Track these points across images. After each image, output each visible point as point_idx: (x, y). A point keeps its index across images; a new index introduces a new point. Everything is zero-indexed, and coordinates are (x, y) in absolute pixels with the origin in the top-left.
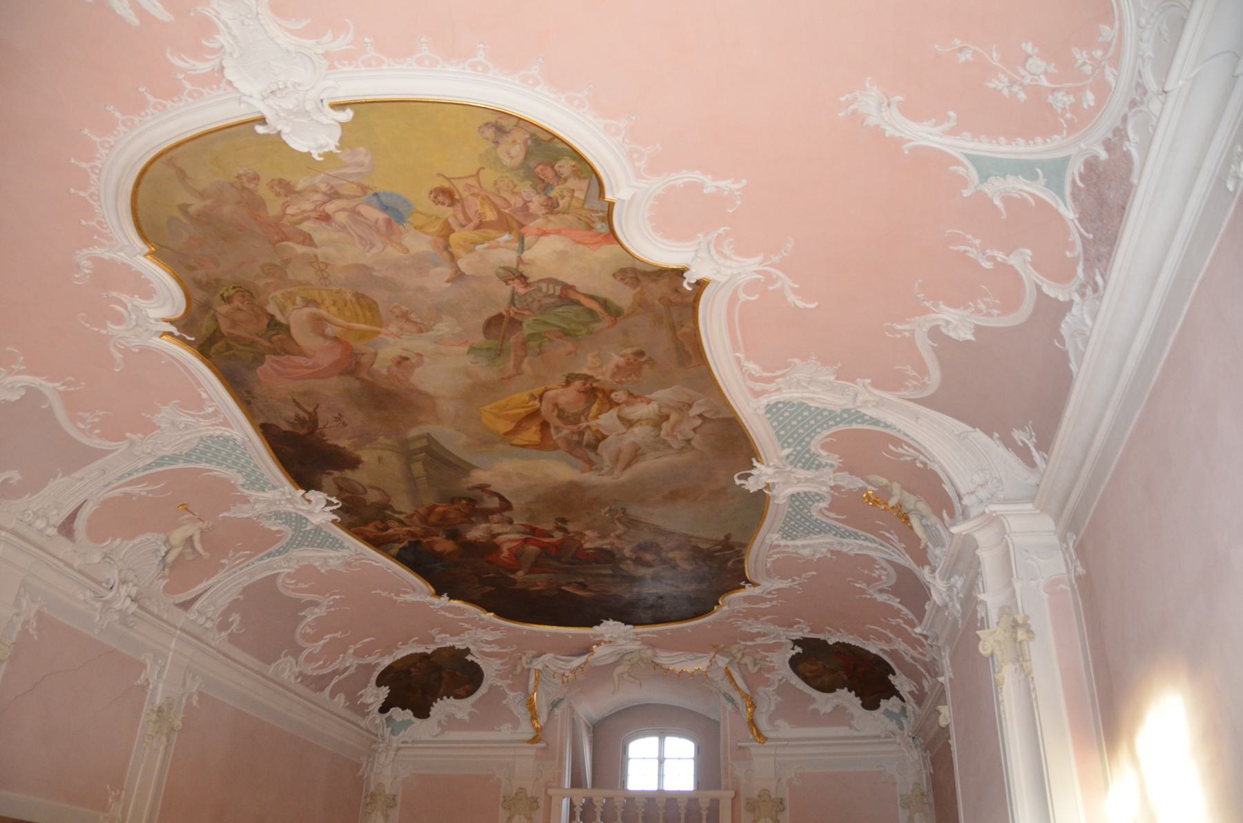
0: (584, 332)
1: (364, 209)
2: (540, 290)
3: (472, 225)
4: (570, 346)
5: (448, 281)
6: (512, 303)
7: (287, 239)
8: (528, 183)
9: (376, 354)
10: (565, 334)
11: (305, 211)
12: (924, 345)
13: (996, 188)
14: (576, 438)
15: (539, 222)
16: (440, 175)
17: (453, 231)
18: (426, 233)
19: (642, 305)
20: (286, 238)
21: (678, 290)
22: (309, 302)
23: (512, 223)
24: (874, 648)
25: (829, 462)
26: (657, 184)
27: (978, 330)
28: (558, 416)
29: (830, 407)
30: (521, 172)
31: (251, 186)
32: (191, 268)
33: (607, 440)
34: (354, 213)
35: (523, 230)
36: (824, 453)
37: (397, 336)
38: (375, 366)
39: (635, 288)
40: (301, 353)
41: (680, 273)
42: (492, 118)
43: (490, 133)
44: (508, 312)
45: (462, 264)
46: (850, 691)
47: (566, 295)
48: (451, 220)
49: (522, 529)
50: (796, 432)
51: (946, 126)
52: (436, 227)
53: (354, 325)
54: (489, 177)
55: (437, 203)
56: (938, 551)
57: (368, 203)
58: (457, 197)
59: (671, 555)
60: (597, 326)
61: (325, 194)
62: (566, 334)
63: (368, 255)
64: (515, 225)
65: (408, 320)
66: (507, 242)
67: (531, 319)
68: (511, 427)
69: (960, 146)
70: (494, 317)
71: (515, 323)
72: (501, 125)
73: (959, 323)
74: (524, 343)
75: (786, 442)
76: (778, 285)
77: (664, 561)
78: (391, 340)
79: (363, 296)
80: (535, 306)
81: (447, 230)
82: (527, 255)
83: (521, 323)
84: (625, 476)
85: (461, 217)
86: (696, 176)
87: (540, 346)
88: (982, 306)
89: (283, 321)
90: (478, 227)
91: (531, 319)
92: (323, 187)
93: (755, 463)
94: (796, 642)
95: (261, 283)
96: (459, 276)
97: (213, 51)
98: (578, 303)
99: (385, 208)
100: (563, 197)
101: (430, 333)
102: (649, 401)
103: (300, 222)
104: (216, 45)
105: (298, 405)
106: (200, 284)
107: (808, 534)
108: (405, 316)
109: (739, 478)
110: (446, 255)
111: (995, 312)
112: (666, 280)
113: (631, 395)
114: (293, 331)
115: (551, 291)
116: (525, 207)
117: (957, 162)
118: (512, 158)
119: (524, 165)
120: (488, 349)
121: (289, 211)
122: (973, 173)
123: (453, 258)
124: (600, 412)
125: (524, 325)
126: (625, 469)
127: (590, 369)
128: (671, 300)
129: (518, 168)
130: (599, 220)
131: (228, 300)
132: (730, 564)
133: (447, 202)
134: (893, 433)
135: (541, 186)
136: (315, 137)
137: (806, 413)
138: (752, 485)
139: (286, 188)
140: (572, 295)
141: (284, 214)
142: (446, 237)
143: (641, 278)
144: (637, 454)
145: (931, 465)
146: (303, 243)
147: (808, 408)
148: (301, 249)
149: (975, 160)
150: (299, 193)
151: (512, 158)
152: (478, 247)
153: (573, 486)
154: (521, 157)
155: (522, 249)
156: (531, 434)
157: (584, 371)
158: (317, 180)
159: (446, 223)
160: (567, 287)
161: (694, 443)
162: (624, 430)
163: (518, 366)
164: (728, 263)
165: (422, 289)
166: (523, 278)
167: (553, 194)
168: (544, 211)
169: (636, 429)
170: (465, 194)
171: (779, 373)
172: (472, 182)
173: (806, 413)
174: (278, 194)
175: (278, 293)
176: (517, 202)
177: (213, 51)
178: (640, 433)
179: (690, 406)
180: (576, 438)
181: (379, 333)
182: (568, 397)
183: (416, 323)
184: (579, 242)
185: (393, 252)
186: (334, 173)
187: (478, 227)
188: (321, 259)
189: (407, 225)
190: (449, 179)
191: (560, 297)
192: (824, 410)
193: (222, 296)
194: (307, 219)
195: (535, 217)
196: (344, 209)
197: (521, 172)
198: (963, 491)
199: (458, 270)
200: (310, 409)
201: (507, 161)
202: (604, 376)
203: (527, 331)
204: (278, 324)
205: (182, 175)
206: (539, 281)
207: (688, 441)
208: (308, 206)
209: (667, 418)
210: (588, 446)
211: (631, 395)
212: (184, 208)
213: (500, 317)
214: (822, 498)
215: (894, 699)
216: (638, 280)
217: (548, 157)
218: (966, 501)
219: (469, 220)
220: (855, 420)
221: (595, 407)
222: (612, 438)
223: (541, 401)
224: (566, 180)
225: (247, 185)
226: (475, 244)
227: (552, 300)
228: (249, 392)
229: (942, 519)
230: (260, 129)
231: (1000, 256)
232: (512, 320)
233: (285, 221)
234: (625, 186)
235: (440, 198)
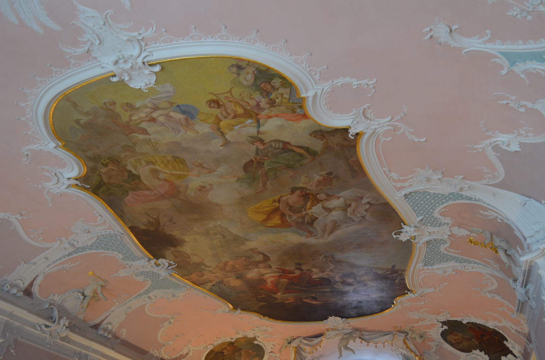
1: (172, 114)
2: (271, 146)
3: (231, 117)
4: (291, 173)
5: (221, 146)
6: (257, 153)
7: (134, 132)
8: (258, 93)
9: (187, 186)
10: (289, 167)
11: (141, 118)
12: (492, 156)
13: (520, 68)
14: (301, 220)
16: (210, 93)
17: (222, 121)
18: (207, 123)
19: (327, 148)
20: (134, 132)
21: (346, 139)
22: (148, 163)
23: (252, 113)
24: (491, 325)
25: (446, 221)
26: (327, 86)
27: (521, 145)
28: (290, 210)
29: (441, 192)
30: (254, 87)
31: (112, 108)
32: (84, 151)
33: (318, 220)
34: (168, 116)
35: (259, 117)
36: (442, 218)
37: (198, 176)
38: (188, 192)
39: (323, 140)
40: (148, 189)
41: (345, 130)
42: (235, 62)
43: (234, 70)
44: (256, 159)
45: (228, 137)
46: (481, 351)
47: (286, 147)
48: (219, 115)
49: (277, 270)
50: (424, 207)
51: (486, 38)
52: (212, 119)
53: (174, 172)
54: (236, 92)
55: (210, 107)
56: (518, 269)
57: (174, 111)
58: (221, 103)
59: (362, 279)
60: (305, 162)
61: (151, 108)
63: (178, 137)
64: (253, 114)
65: (203, 167)
66: (250, 123)
68: (265, 217)
69: (495, 48)
71: (260, 164)
72: (239, 65)
73: (510, 141)
74: (266, 174)
75: (419, 212)
76: (402, 131)
77: (359, 282)
79: (178, 158)
81: (218, 121)
82: (262, 129)
83: (263, 163)
84: (331, 238)
85: (224, 113)
86: (347, 80)
88: (522, 132)
89: (136, 173)
90: (234, 117)
92: (150, 105)
93: (403, 226)
94: (444, 323)
95: (122, 155)
96: (227, 143)
97: (84, 43)
99: (183, 112)
100: (277, 98)
101: (215, 173)
102: (338, 198)
103: (140, 123)
104: (86, 39)
105: (148, 215)
106: (89, 158)
107: (440, 262)
108: (201, 166)
109: (395, 234)
110: (218, 132)
111: (530, 134)
113: (328, 195)
114: (142, 178)
115: (277, 146)
116: (258, 104)
117: (496, 57)
118: (248, 81)
119: (254, 84)
121: (133, 118)
122: (505, 62)
123: (223, 134)
124: (312, 206)
125: (265, 165)
126: (330, 234)
127: (304, 184)
128: (341, 145)
129: (251, 86)
130: (297, 108)
131: (106, 165)
132: (397, 281)
133: (216, 106)
134: (481, 204)
135: (264, 94)
136: (143, 81)
137: (428, 197)
138: (403, 237)
139: (130, 107)
140: (289, 147)
141: (131, 120)
142: (218, 124)
143: (325, 135)
144: (335, 226)
145: (506, 221)
146: (142, 133)
147: (429, 194)
148: (141, 137)
149: (505, 54)
150: (136, 109)
151: (248, 81)
152: (236, 128)
153: (302, 245)
154: (252, 80)
155: (259, 126)
156: (276, 220)
157: (301, 185)
158: (146, 102)
159: (217, 117)
160: (285, 143)
161: (367, 218)
162: (326, 213)
163: (264, 185)
164: (372, 123)
166: (261, 141)
167: (272, 97)
168: (268, 106)
169: (334, 213)
170: (225, 102)
171: (409, 177)
172: (228, 95)
173: (428, 197)
174: (126, 111)
175: (132, 160)
176: (253, 103)
177: (84, 43)
178: (336, 215)
179: (362, 198)
180: (301, 220)
181: (188, 175)
182: (293, 199)
183: (207, 168)
185: (190, 134)
186: (154, 97)
187: (234, 118)
188: (153, 141)
189: (197, 120)
190: (216, 95)
191: (282, 149)
192: (439, 194)
193: (102, 163)
194: (143, 121)
195: (264, 109)
196: (162, 115)
197: (254, 87)
198: (526, 235)
199: (226, 140)
200: (155, 217)
201: (245, 83)
202: (312, 187)
203: (267, 167)
204: (134, 175)
205: (75, 105)
207: (364, 217)
208: (143, 115)
209: (350, 205)
210: (308, 224)
211: (328, 195)
212: (77, 122)
213: (252, 161)
214: (445, 242)
215: (510, 356)
216: (324, 136)
217: (266, 78)
218: (529, 241)
220: (457, 198)
221: (309, 204)
222: (321, 218)
223: (279, 203)
224: (278, 89)
225: (110, 107)
226: (234, 126)
227: (279, 151)
228: (122, 211)
229: (517, 251)
230: (115, 79)
231: (529, 105)
233: (131, 123)
234: (310, 90)
235: (212, 105)
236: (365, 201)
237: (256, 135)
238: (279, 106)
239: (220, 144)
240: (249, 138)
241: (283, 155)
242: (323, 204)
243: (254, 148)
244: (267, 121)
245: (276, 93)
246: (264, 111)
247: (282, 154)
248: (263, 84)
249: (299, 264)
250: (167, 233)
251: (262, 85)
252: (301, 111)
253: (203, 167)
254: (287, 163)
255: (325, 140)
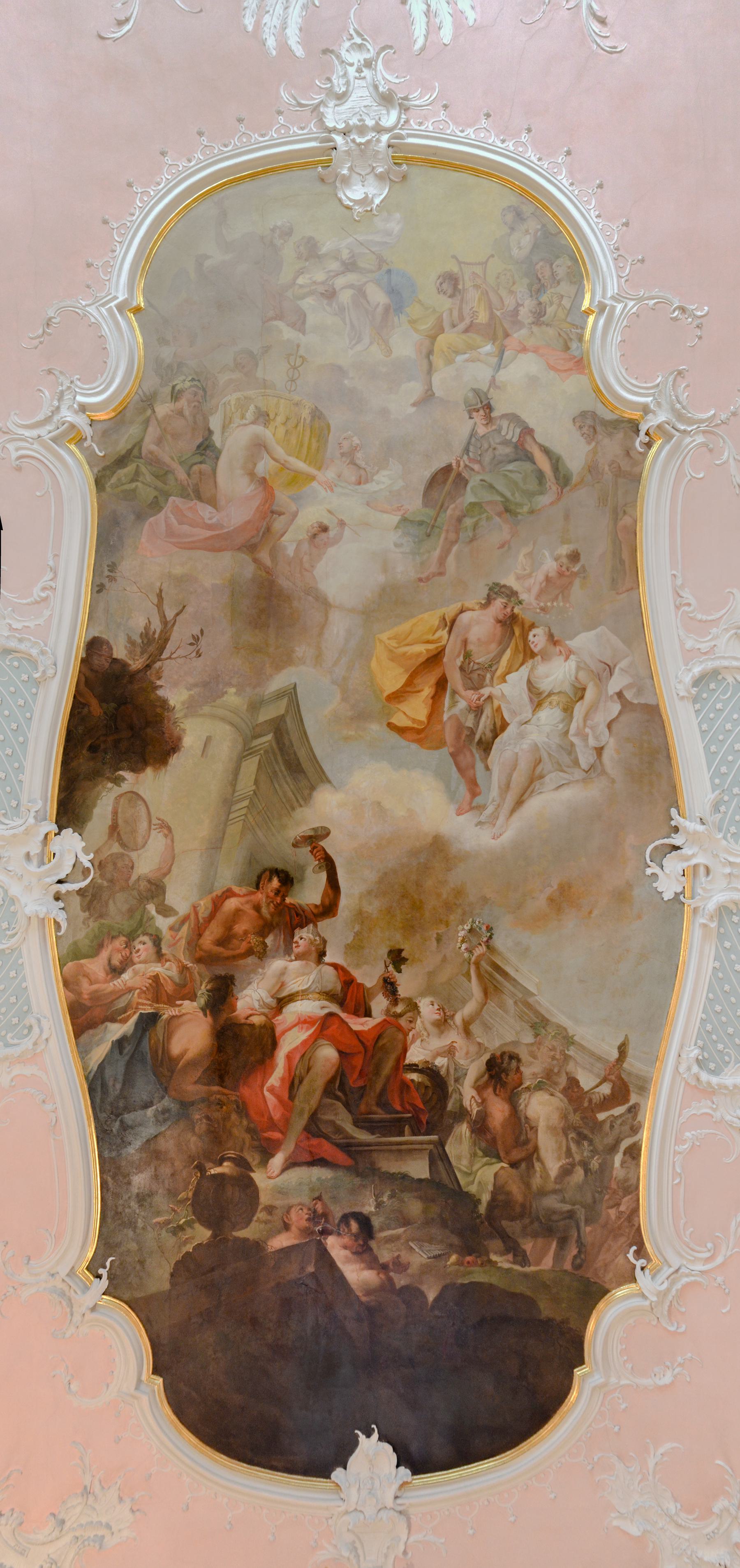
0: (526, 509)
2: (499, 431)
3: (462, 326)
5: (414, 405)
6: (467, 450)
9: (295, 515)
10: (508, 510)
15: (524, 332)
35: (507, 342)
37: (330, 487)
38: (283, 539)
44: (458, 463)
55: (440, 291)
60: (544, 500)
62: (507, 510)
64: (500, 333)
65: (353, 463)
66: (487, 354)
67: (479, 477)
70: (442, 469)
71: (461, 481)
78: (323, 493)
80: (487, 458)
82: (503, 376)
83: (466, 482)
85: (456, 313)
87: (475, 526)
89: (218, 444)
90: (466, 331)
91: (479, 477)
93: (677, 820)
98: (530, 458)
100: (551, 304)
110: (425, 363)
112: (620, 435)
115: (508, 437)
116: (515, 312)
120: (421, 523)
123: (430, 370)
126: (513, 811)
143: (598, 428)
152: (460, 358)
155: (498, 367)
159: (440, 320)
160: (528, 431)
163: (442, 561)
165: (384, 412)
166: (489, 408)
168: (530, 320)
170: (469, 284)
181: (313, 478)
183: (359, 467)
184: (552, 368)
187: (466, 331)
199: (430, 388)
203: (469, 497)
206: (504, 416)
213: (448, 469)
219: (462, 318)
224: (558, 283)
226: (457, 352)
227: (508, 450)
228: (113, 567)
232: (459, 475)
236: (616, 684)
237: (485, 390)
238: (547, 325)
239: (414, 398)
240: (471, 395)
241: (511, 467)
242: (532, 669)
243: (464, 430)
244: (515, 358)
245: (552, 290)
246: (520, 329)
247: (510, 462)
248: (541, 264)
249: (397, 958)
250: (160, 693)
251: (538, 267)
252: (578, 347)
253: (353, 463)
254: (508, 494)
255: (593, 444)
